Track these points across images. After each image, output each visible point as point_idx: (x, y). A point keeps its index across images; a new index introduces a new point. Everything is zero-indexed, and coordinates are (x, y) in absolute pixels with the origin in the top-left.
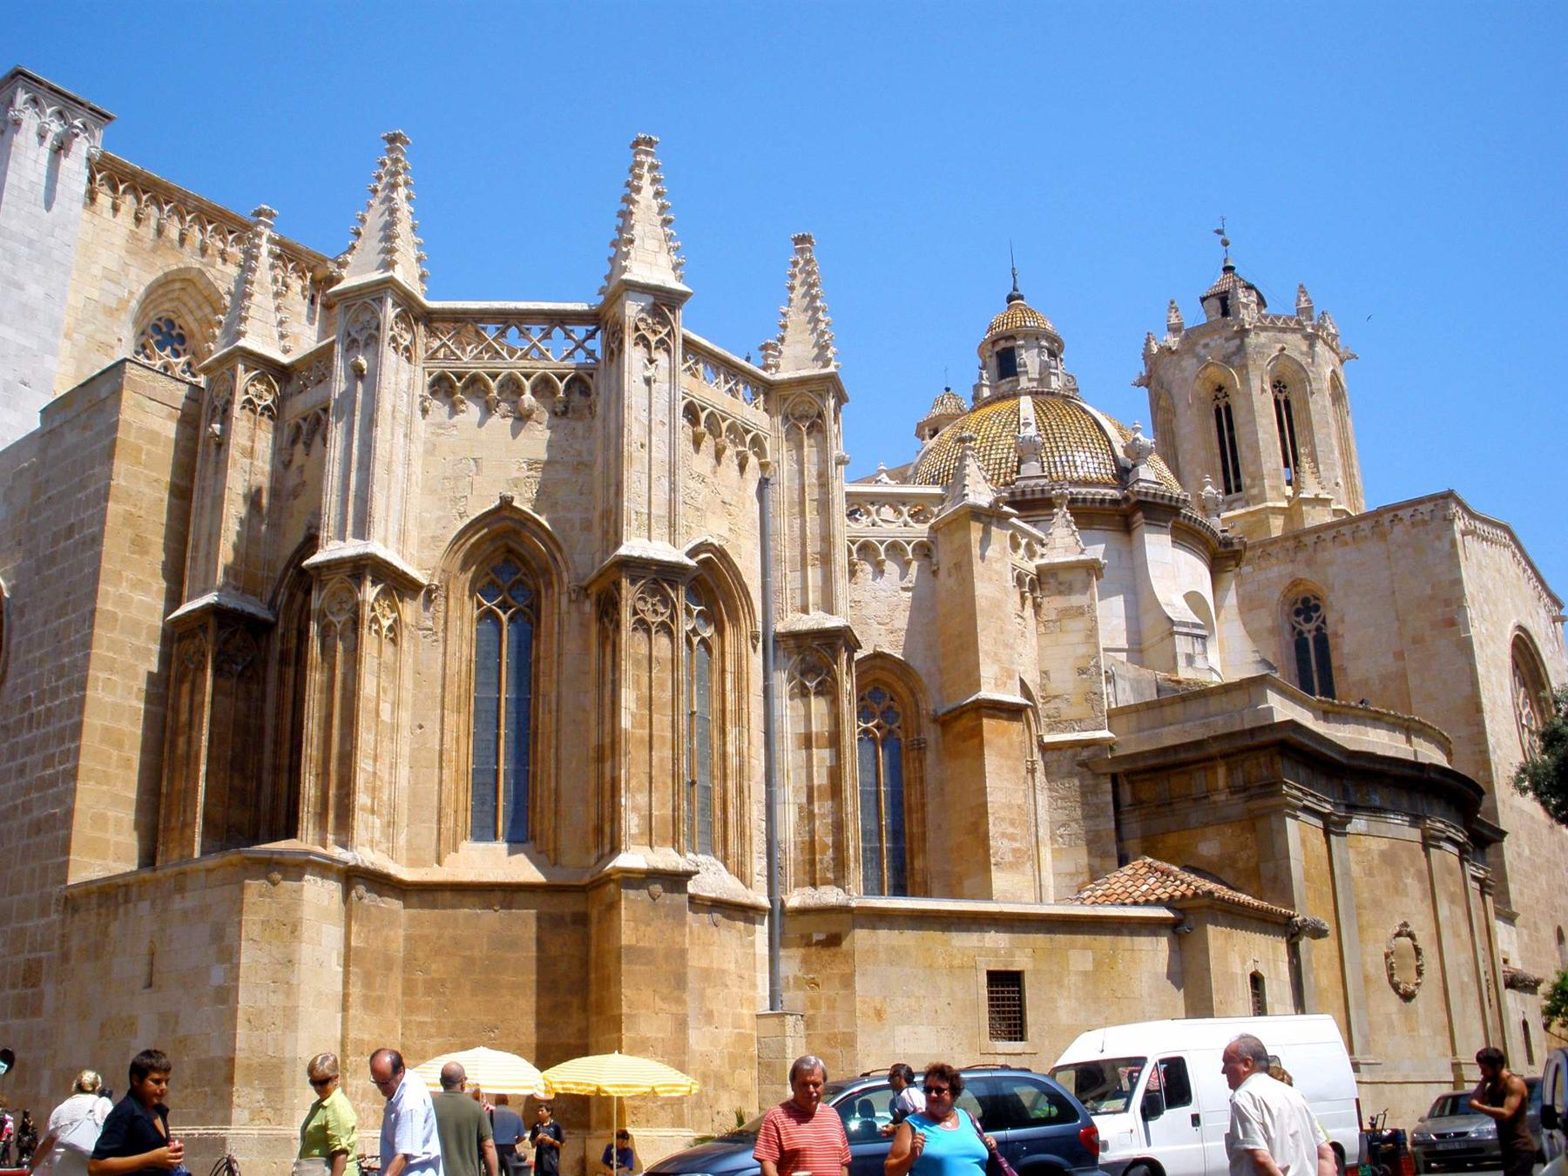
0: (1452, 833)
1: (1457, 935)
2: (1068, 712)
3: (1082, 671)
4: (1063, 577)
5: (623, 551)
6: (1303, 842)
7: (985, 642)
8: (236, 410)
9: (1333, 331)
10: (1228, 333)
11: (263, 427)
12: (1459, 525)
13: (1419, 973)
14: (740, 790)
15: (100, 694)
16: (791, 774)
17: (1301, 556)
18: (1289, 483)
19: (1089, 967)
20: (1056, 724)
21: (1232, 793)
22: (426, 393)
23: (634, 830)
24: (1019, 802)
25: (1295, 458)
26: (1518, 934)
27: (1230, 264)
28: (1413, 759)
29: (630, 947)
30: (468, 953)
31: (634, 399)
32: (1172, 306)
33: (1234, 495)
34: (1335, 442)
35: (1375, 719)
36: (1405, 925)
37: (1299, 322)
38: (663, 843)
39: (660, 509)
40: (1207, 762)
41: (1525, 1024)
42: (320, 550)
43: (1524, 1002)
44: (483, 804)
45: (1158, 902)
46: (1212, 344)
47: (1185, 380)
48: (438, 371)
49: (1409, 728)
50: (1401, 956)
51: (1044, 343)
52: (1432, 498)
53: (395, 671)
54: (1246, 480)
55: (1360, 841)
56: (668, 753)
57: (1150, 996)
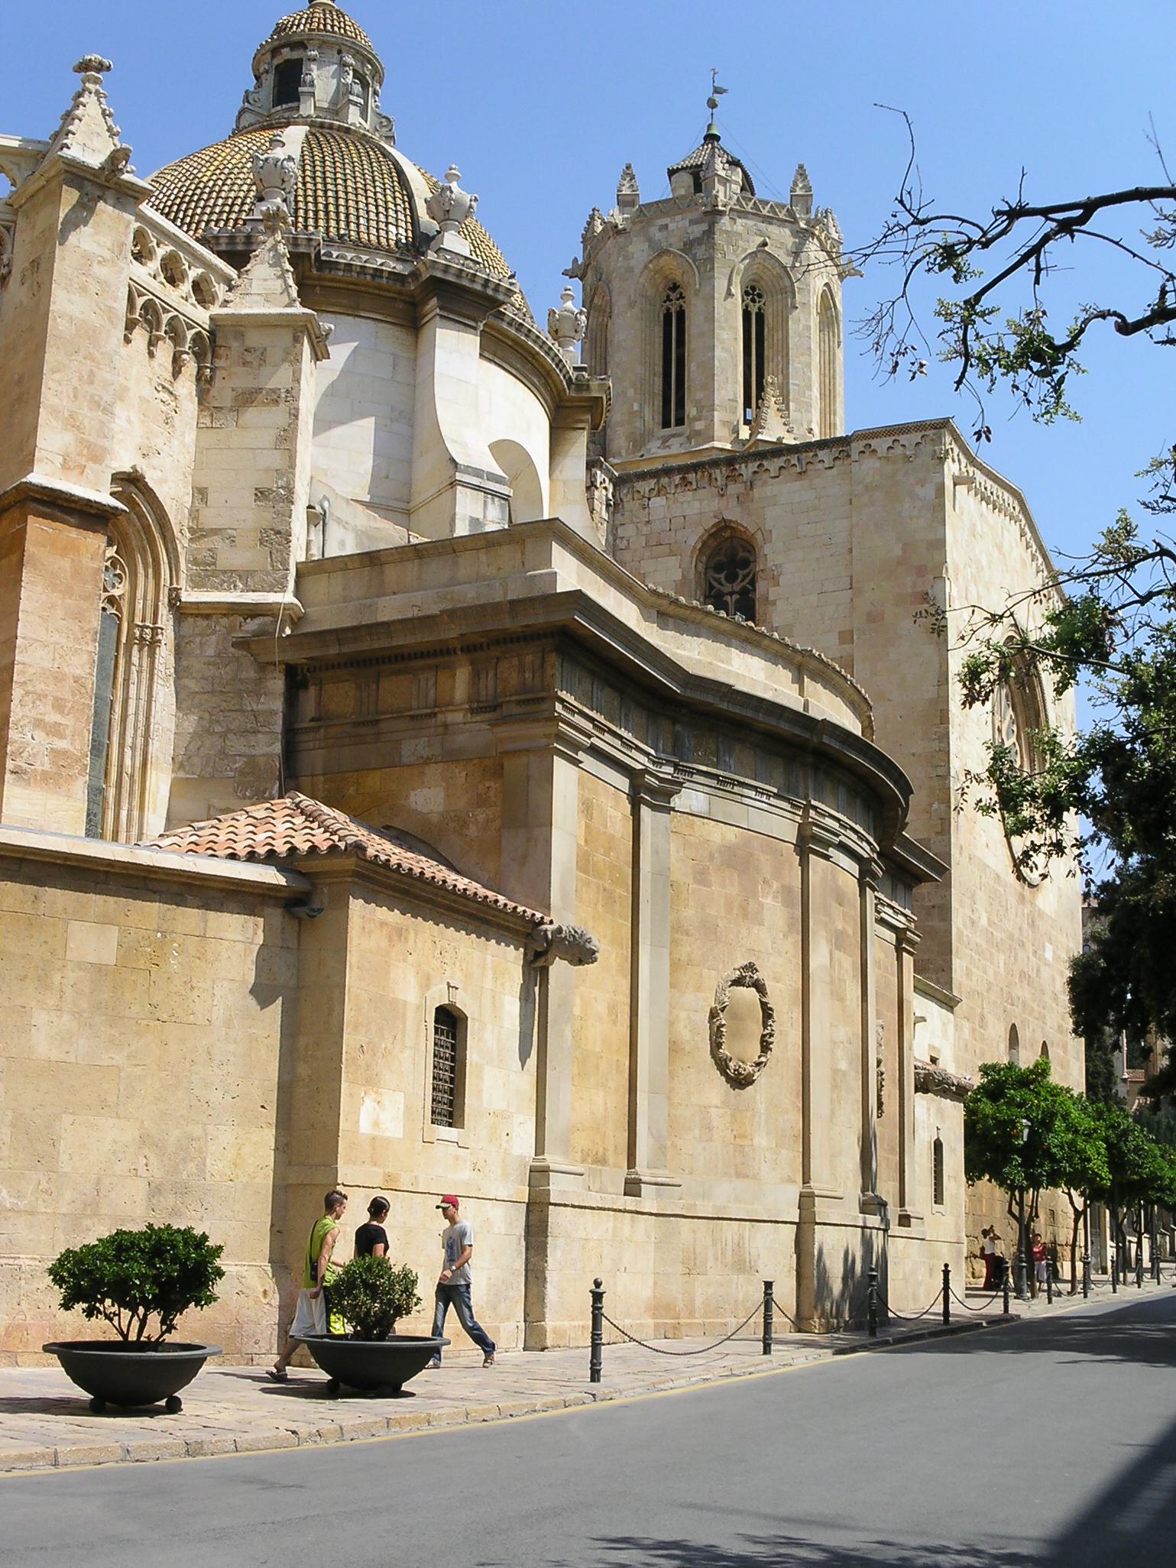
0: (849, 839)
1: (838, 996)
2: (231, 558)
3: (261, 494)
4: (254, 339)
6: (587, 808)
9: (835, 236)
10: (695, 215)
12: (951, 468)
13: (765, 1047)
17: (734, 489)
18: (747, 422)
19: (109, 957)
20: (207, 573)
21: (473, 711)
24: (79, 672)
25: (761, 388)
26: (956, 1025)
27: (714, 131)
28: (801, 710)
32: (628, 173)
33: (673, 429)
34: (815, 376)
35: (746, 640)
36: (751, 967)
37: (790, 213)
40: (438, 656)
41: (938, 1146)
43: (940, 1112)
45: (271, 858)
46: (671, 226)
47: (630, 270)
49: (802, 665)
50: (736, 1017)
51: (349, 59)
52: (919, 426)
54: (691, 410)
55: (692, 826)
57: (228, 1023)
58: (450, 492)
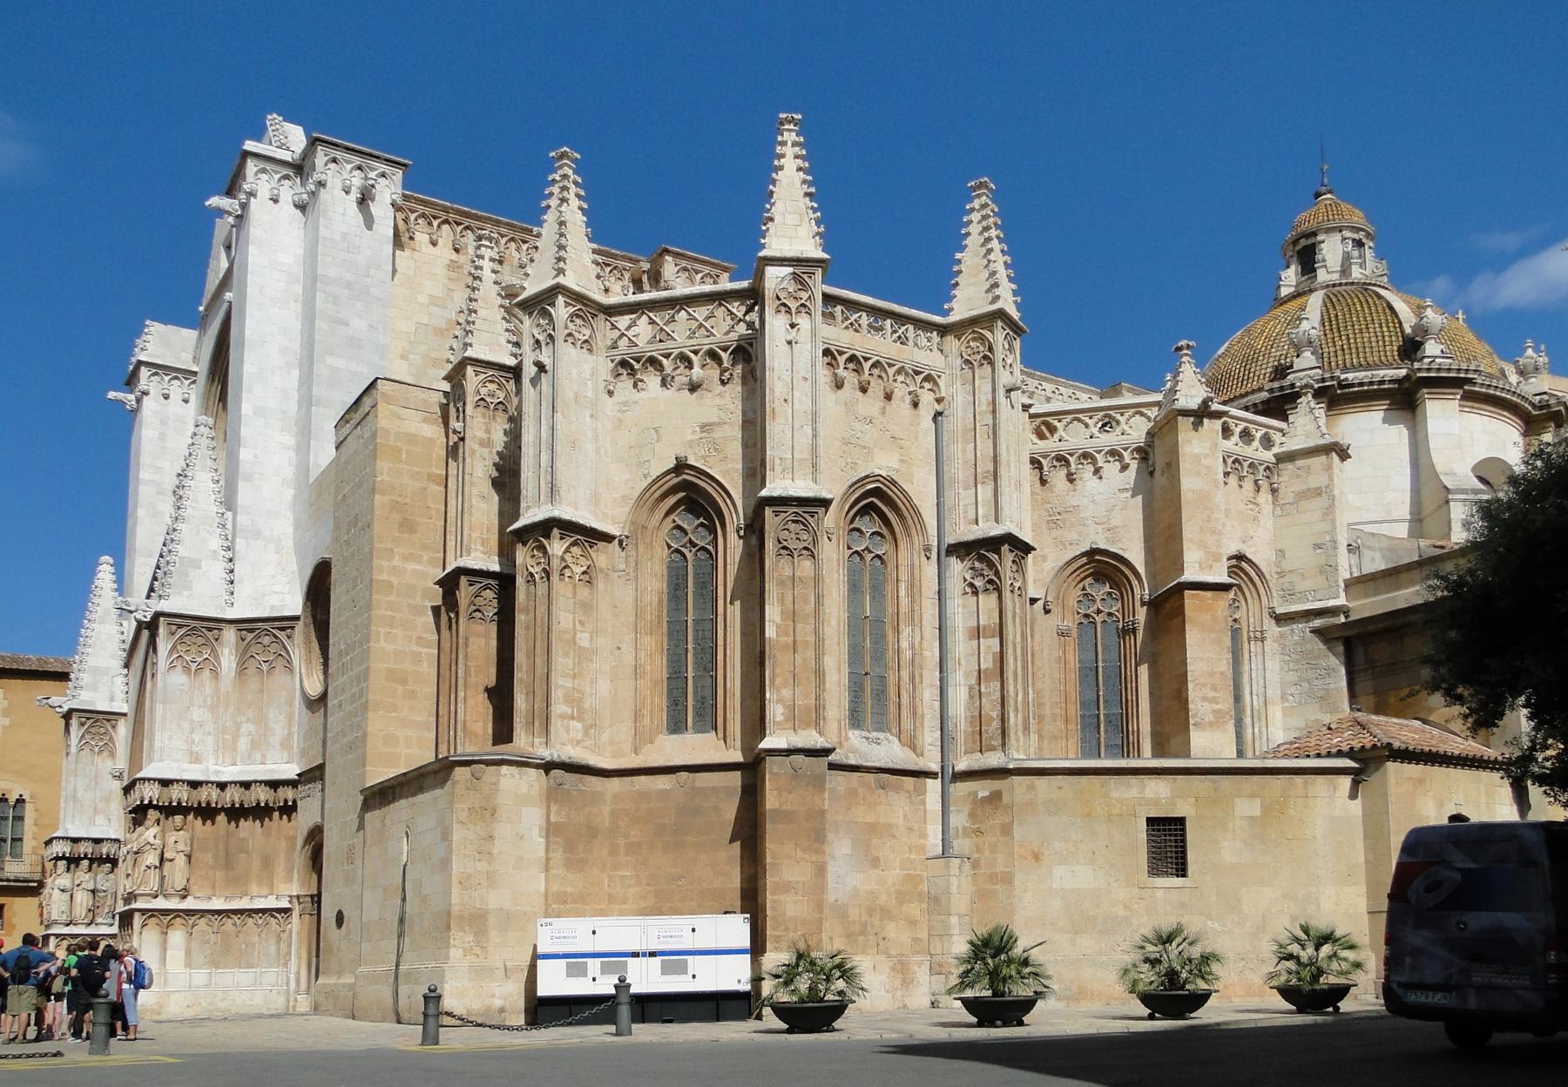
5: (764, 493)
7: (1189, 531)
8: (469, 409)
11: (498, 419)
14: (912, 678)
15: (383, 644)
16: (962, 661)
22: (610, 378)
23: (779, 718)
29: (773, 811)
30: (659, 821)
31: (776, 361)
38: (807, 725)
39: (803, 453)
42: (521, 518)
44: (677, 705)
48: (618, 358)
53: (586, 607)
56: (811, 654)
58: (1445, 508)
